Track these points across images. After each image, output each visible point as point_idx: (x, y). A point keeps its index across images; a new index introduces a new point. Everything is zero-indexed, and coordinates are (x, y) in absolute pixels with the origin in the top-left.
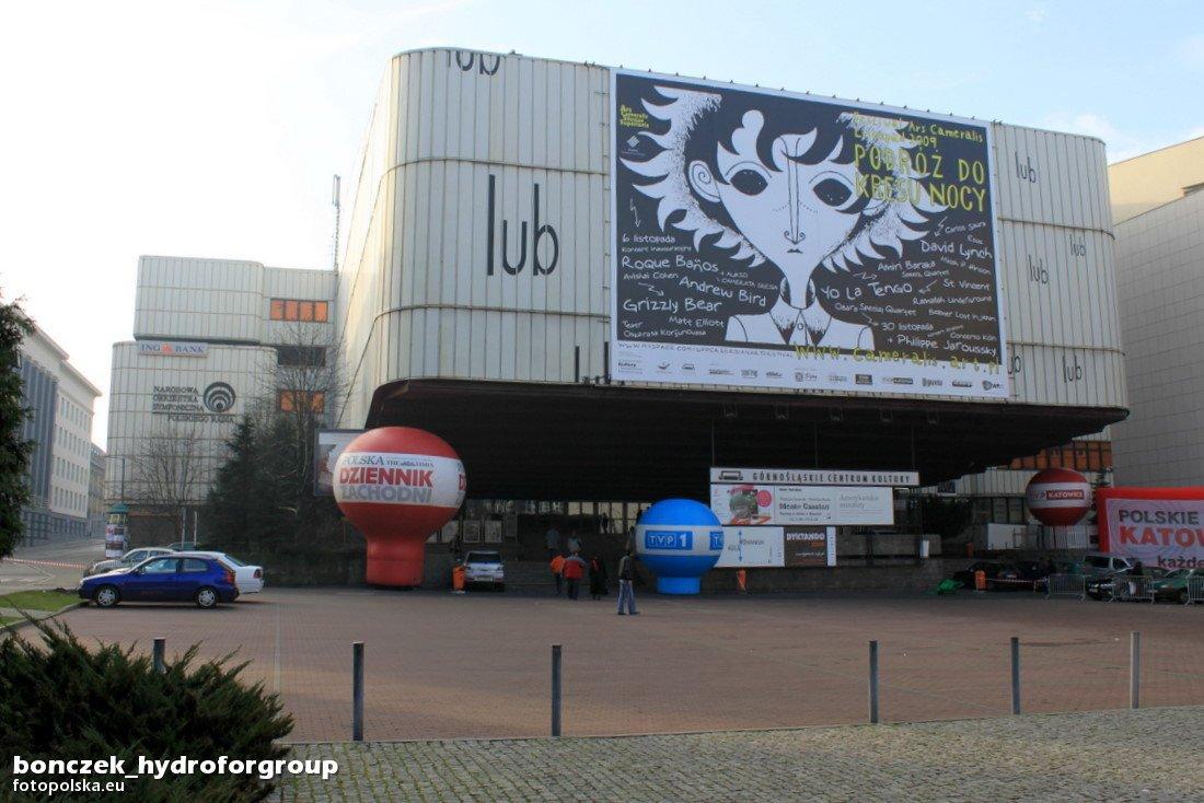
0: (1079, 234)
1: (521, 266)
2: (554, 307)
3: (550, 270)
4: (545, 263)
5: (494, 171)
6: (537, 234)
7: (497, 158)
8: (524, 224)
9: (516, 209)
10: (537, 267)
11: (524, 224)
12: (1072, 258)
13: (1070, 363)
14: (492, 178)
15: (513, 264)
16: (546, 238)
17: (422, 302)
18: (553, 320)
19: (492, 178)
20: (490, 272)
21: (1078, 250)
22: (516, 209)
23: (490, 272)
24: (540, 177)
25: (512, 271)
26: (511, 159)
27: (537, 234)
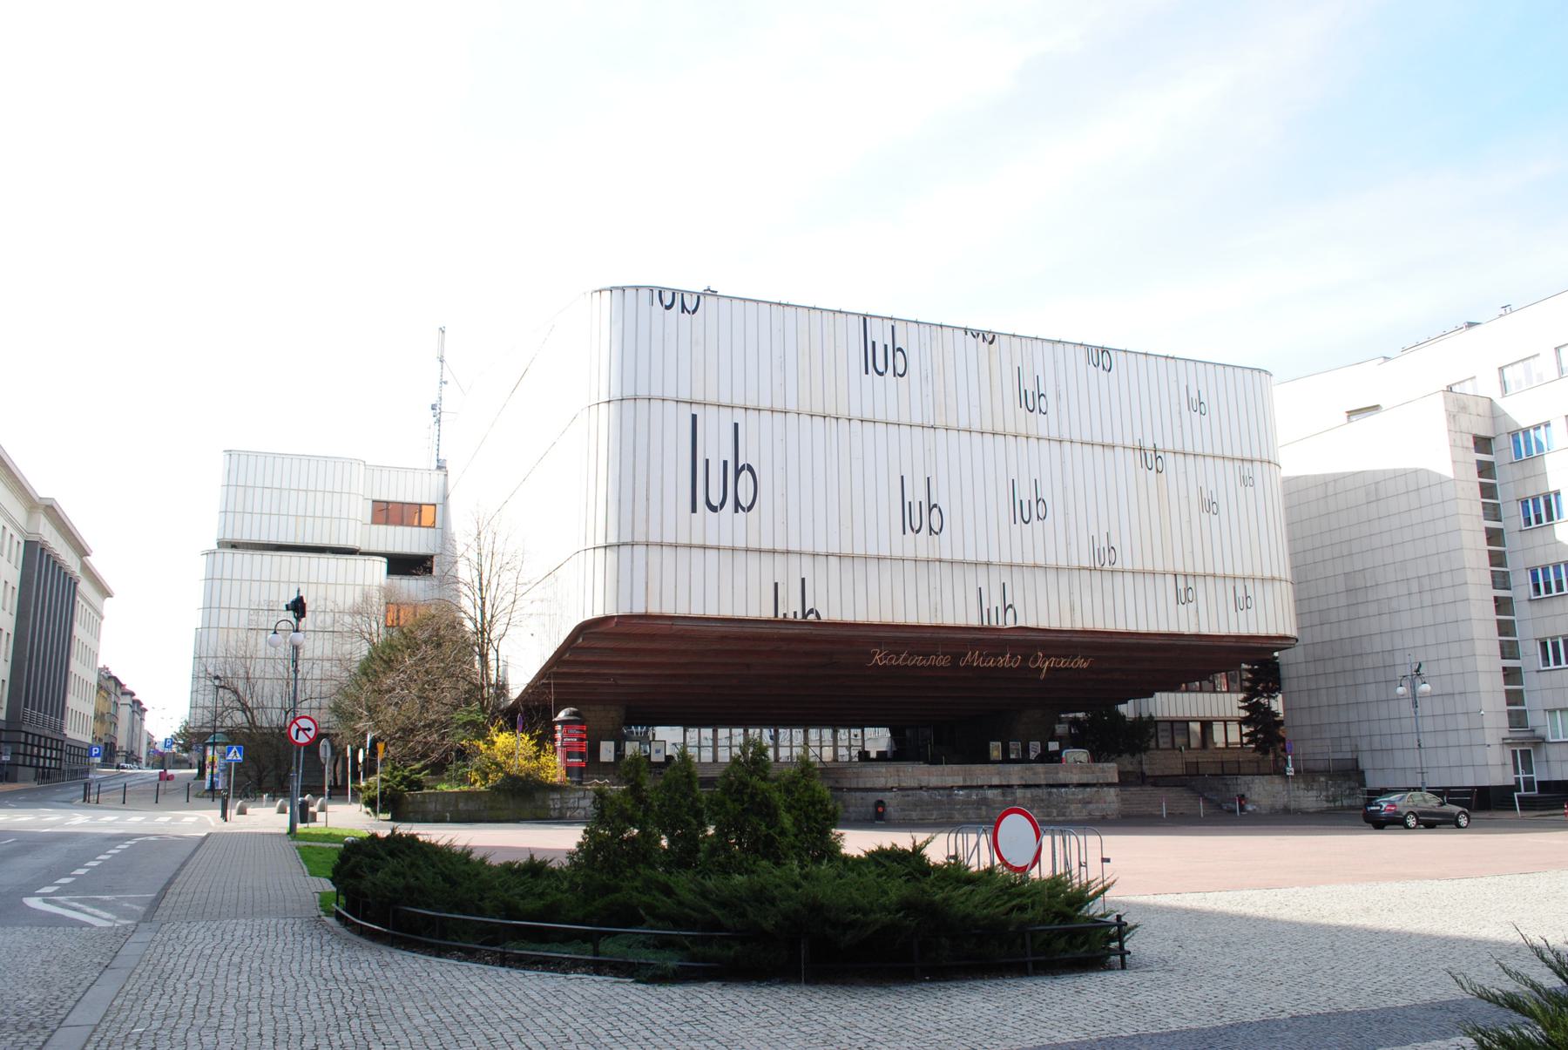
0: (1247, 465)
1: (722, 504)
2: (753, 544)
3: (750, 508)
4: (745, 502)
5: (696, 410)
6: (738, 473)
7: (699, 397)
8: (725, 463)
9: (716, 449)
10: (737, 504)
11: (725, 463)
12: (1241, 490)
13: (1241, 593)
14: (694, 417)
15: (715, 502)
16: (745, 475)
17: (629, 540)
18: (753, 557)
19: (694, 417)
20: (694, 510)
21: (1247, 481)
22: (716, 449)
23: (694, 510)
24: (739, 416)
25: (714, 509)
26: (712, 398)
27: (738, 473)
